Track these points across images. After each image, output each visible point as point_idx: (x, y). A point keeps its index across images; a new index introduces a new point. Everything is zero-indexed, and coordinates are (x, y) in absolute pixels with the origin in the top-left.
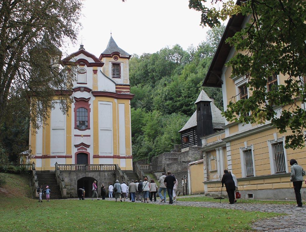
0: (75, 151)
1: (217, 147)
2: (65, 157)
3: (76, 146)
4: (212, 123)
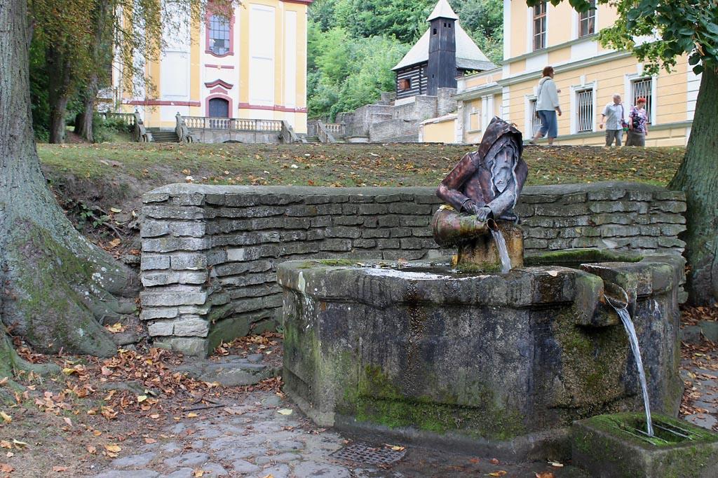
0: (206, 94)
1: (484, 94)
2: (189, 104)
3: (208, 85)
4: (454, 58)
